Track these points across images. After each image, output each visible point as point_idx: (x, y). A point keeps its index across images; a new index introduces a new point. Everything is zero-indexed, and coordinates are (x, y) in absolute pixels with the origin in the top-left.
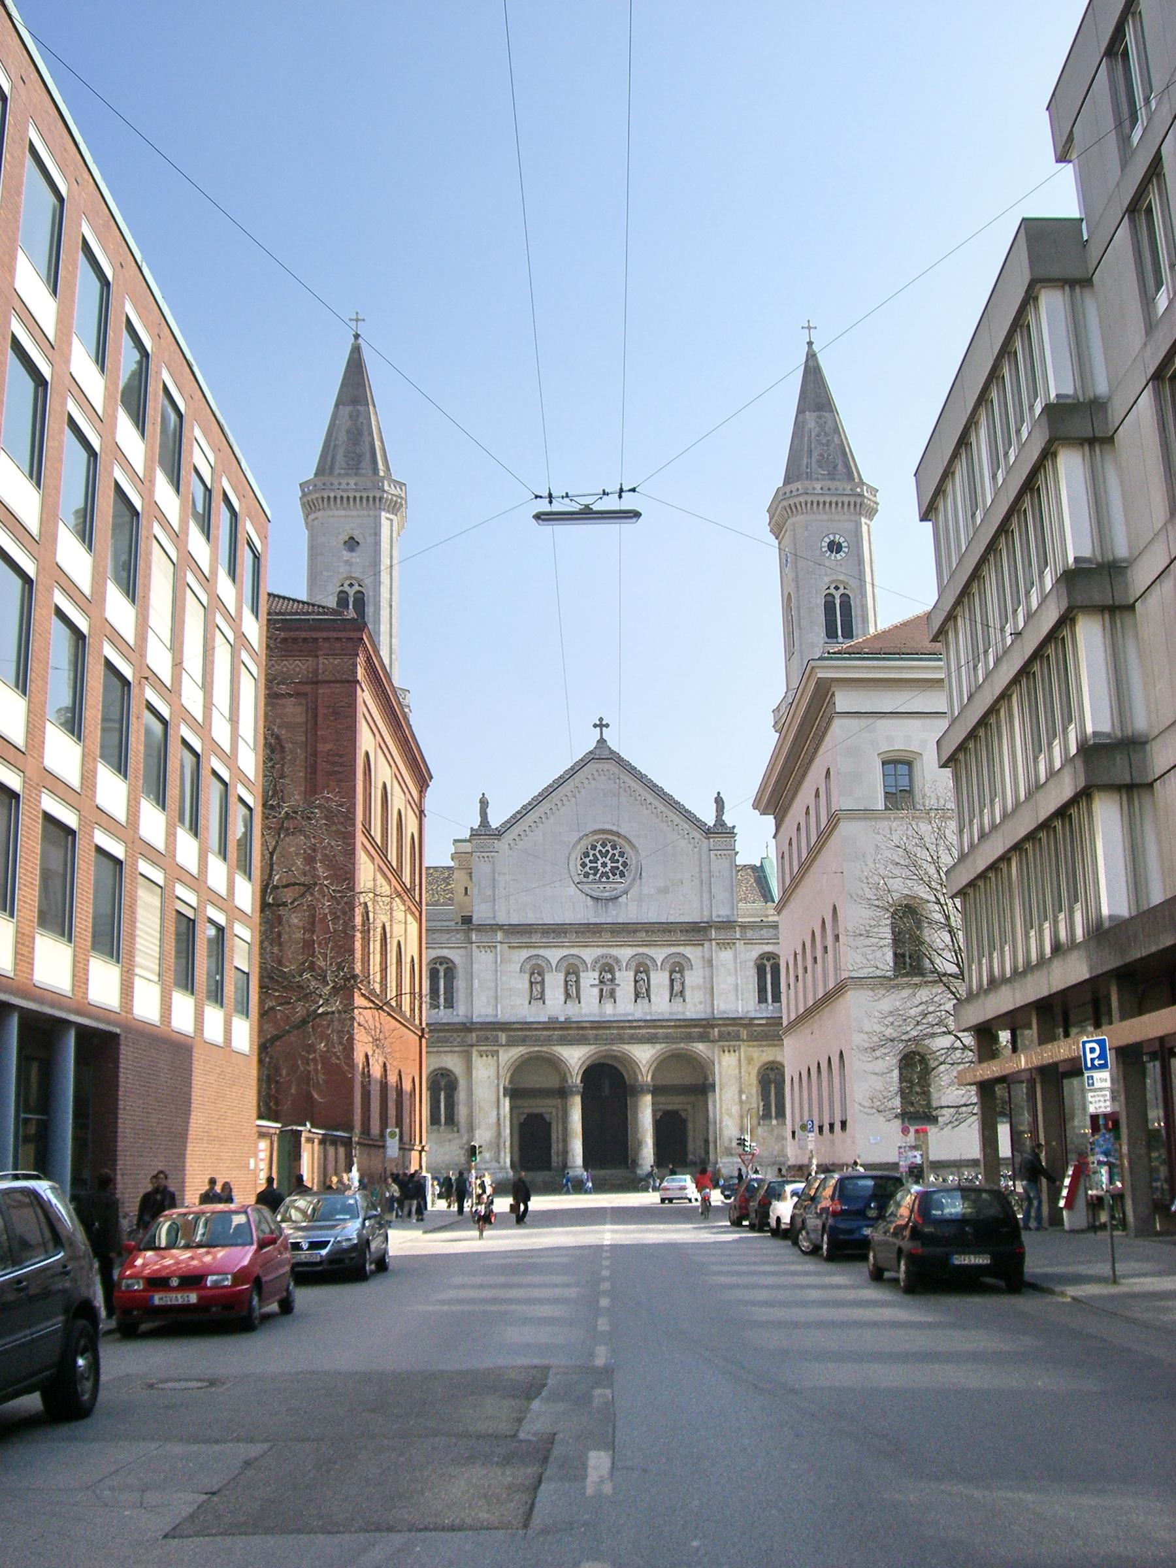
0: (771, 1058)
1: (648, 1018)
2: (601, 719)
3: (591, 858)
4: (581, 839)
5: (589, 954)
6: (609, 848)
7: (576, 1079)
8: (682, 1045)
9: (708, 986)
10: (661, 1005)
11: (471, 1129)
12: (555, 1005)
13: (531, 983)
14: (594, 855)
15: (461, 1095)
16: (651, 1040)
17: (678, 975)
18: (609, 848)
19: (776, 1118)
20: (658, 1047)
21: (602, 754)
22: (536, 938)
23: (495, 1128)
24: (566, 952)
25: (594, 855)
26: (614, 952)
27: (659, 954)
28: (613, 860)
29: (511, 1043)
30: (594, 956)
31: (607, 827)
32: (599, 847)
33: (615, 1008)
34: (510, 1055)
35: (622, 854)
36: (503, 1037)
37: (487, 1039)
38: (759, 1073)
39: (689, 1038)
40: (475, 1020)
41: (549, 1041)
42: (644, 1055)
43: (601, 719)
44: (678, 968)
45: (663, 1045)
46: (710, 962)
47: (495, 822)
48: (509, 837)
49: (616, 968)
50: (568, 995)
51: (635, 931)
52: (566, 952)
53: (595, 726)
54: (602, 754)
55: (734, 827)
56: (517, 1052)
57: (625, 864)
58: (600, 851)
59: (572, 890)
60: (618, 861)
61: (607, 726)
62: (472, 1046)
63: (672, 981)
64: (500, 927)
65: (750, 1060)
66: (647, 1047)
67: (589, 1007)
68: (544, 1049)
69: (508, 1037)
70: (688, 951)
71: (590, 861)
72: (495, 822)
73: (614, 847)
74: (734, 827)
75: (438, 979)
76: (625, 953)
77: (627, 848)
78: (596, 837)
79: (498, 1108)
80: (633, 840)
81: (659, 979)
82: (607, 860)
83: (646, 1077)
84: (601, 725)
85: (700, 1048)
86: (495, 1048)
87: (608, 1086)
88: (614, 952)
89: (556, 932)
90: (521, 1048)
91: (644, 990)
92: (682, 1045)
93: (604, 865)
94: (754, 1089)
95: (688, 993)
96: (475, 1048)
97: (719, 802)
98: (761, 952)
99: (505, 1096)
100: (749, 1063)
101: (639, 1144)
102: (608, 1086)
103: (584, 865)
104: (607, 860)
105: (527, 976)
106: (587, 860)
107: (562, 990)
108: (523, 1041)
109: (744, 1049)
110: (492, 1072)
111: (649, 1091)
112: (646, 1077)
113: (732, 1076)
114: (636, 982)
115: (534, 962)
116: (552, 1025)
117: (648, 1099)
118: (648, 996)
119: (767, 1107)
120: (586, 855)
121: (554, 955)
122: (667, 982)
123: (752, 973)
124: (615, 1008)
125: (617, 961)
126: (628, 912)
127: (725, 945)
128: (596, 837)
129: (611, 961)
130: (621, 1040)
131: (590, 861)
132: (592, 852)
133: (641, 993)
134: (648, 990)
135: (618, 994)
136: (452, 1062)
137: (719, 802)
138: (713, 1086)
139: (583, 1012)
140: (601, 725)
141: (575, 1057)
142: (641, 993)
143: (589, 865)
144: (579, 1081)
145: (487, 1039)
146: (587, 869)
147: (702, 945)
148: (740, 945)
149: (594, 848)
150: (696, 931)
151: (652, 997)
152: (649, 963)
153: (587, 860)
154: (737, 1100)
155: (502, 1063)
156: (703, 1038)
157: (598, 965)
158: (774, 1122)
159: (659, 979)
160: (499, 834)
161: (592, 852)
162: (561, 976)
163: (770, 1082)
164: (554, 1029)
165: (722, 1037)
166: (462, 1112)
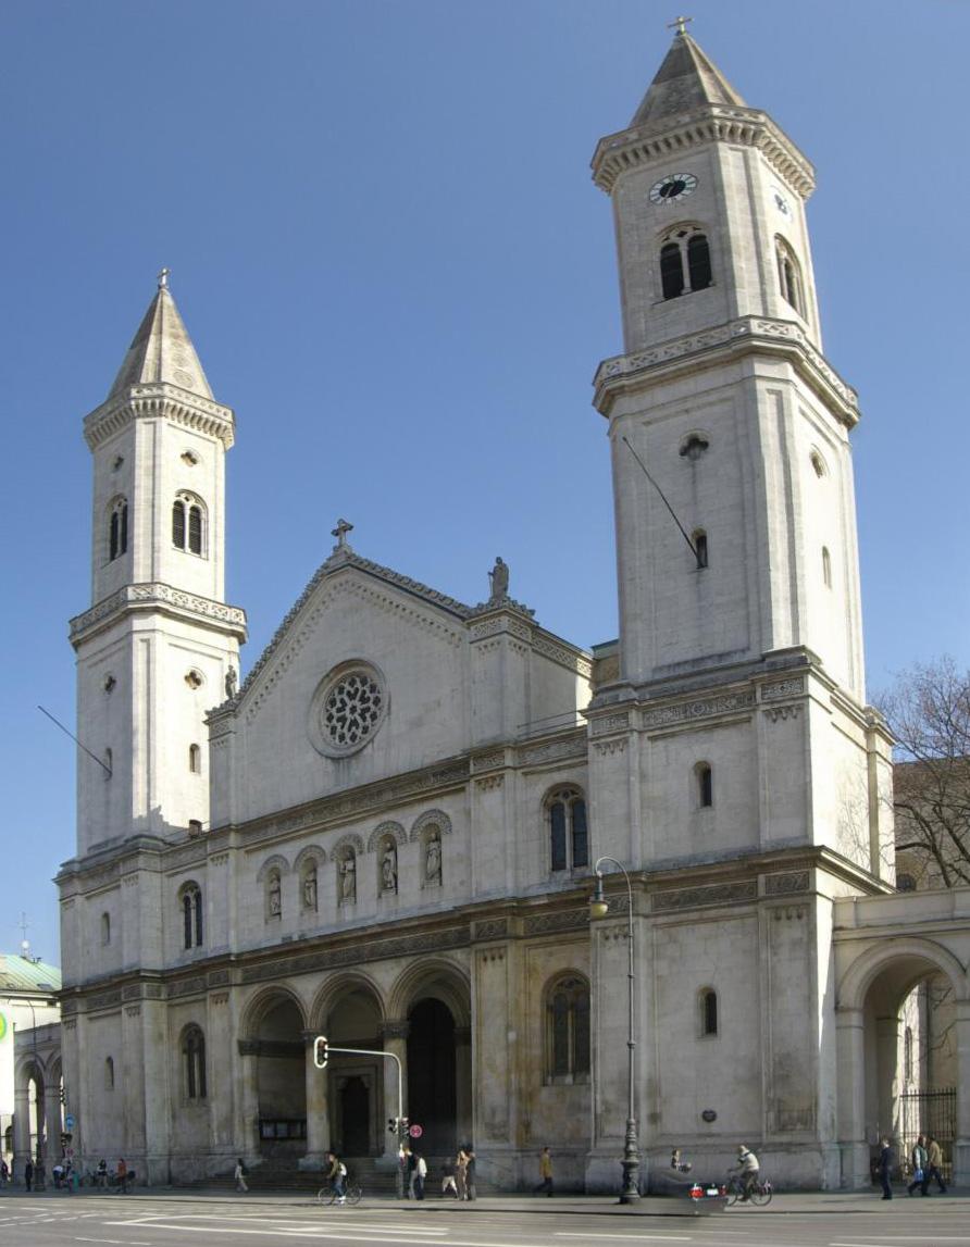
0: (564, 965)
3: (339, 705)
6: (358, 685)
8: (434, 957)
10: (413, 898)
14: (342, 701)
18: (358, 685)
20: (404, 962)
22: (272, 831)
29: (246, 983)
33: (355, 911)
38: (547, 989)
39: (446, 944)
41: (284, 973)
44: (434, 834)
45: (410, 959)
49: (357, 851)
50: (307, 905)
51: (380, 793)
59: (311, 756)
65: (530, 971)
66: (389, 964)
67: (330, 917)
68: (278, 984)
70: (448, 805)
73: (364, 682)
81: (410, 857)
85: (459, 957)
97: (500, 574)
103: (330, 718)
109: (513, 951)
118: (396, 886)
124: (355, 911)
125: (358, 840)
132: (338, 698)
137: (500, 574)
139: (322, 922)
149: (341, 690)
151: (399, 885)
156: (463, 941)
165: (482, 937)
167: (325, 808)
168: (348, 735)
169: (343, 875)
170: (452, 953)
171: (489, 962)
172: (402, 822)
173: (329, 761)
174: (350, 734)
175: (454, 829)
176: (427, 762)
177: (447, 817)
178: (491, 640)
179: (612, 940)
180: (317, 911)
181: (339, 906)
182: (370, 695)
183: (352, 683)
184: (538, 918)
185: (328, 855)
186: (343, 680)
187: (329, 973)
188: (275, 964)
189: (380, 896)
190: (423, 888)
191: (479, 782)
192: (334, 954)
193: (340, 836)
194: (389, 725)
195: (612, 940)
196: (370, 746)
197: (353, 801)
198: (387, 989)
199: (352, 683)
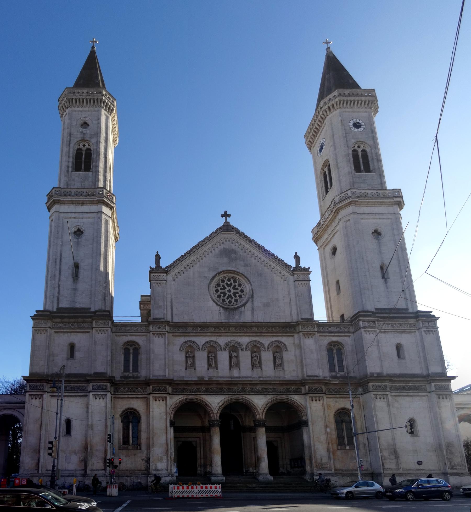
1: (261, 379)
2: (226, 212)
4: (216, 275)
5: (222, 341)
6: (232, 281)
7: (216, 416)
8: (284, 396)
9: (299, 361)
11: (149, 447)
12: (201, 369)
13: (187, 358)
14: (223, 286)
15: (143, 425)
16: (264, 393)
17: (279, 354)
18: (232, 281)
19: (348, 445)
20: (269, 397)
21: (227, 228)
22: (189, 330)
23: (165, 446)
24: (208, 339)
25: (223, 286)
26: (239, 339)
27: (266, 341)
28: (234, 288)
30: (225, 342)
31: (230, 269)
32: (226, 281)
33: (239, 373)
34: (175, 400)
35: (240, 285)
36: (169, 389)
37: (159, 389)
39: (289, 392)
40: (151, 378)
41: (198, 392)
42: (260, 402)
43: (226, 212)
44: (278, 350)
45: (272, 396)
46: (299, 346)
47: (164, 264)
48: (173, 273)
50: (209, 365)
52: (208, 339)
53: (222, 216)
54: (227, 228)
55: (309, 268)
56: (177, 399)
57: (242, 291)
58: (227, 284)
59: (211, 303)
60: (237, 289)
61: (229, 216)
62: (149, 394)
63: (274, 358)
64: (168, 323)
66: (261, 397)
69: (173, 389)
70: (284, 340)
71: (221, 289)
72: (164, 264)
73: (235, 281)
74: (309, 268)
75: (129, 354)
76: (245, 340)
77: (243, 281)
78: (224, 275)
79: (167, 433)
80: (248, 276)
81: (267, 357)
82: (231, 288)
83: (261, 415)
84: (226, 215)
86: (165, 395)
87: (235, 421)
88: (239, 339)
89: (202, 328)
90: (181, 396)
91: (257, 363)
92: (284, 396)
93: (229, 291)
94: (333, 426)
95: (286, 365)
96: (151, 396)
98: (330, 341)
99: (170, 426)
100: (328, 409)
101: (258, 460)
102: (235, 421)
103: (217, 291)
104: (233, 291)
105: (184, 353)
106: (219, 288)
107: (206, 361)
108: (182, 392)
110: (163, 409)
111: (264, 425)
112: (261, 415)
113: (318, 413)
114: (252, 358)
115: (188, 344)
116: (201, 382)
117: (262, 431)
119: (340, 437)
120: (218, 285)
121: (201, 341)
122: (272, 358)
123: (325, 353)
124: (239, 373)
125: (240, 345)
126: (246, 316)
127: (307, 335)
128: (224, 275)
130: (244, 392)
131: (221, 289)
132: (222, 284)
133: (256, 363)
134: (260, 363)
135: (242, 365)
136: (137, 405)
138: (306, 423)
139: (220, 375)
140: (226, 215)
141: (215, 402)
142: (256, 363)
143: (220, 291)
144: (218, 418)
145: (159, 389)
146: (219, 293)
147: (293, 336)
148: (317, 335)
149: (223, 281)
150: (288, 328)
151: (263, 367)
152: (260, 346)
153: (219, 288)
154: (323, 432)
155: (168, 404)
156: (298, 392)
157: (228, 348)
158: (348, 448)
159: (267, 357)
160: (167, 271)
161: (222, 284)
162: (205, 353)
163: (342, 421)
164: (201, 384)
165: (311, 391)
166: (143, 436)
167: (221, 327)
168: (227, 301)
169: (230, 358)
170: (292, 396)
171: (314, 401)
172: (263, 342)
173: (221, 308)
174: (228, 300)
175: (289, 349)
176: (273, 321)
177: (285, 345)
178: (304, 282)
179: (378, 399)
180: (217, 369)
181: (230, 369)
182: (221, 286)
183: (229, 280)
184: (331, 388)
185: (222, 347)
186: (225, 278)
187: (227, 396)
188: (194, 388)
189: (252, 369)
190: (274, 369)
191: (304, 334)
192: (229, 389)
194: (253, 301)
195: (378, 399)
196: (243, 307)
198: (260, 407)
199: (229, 280)
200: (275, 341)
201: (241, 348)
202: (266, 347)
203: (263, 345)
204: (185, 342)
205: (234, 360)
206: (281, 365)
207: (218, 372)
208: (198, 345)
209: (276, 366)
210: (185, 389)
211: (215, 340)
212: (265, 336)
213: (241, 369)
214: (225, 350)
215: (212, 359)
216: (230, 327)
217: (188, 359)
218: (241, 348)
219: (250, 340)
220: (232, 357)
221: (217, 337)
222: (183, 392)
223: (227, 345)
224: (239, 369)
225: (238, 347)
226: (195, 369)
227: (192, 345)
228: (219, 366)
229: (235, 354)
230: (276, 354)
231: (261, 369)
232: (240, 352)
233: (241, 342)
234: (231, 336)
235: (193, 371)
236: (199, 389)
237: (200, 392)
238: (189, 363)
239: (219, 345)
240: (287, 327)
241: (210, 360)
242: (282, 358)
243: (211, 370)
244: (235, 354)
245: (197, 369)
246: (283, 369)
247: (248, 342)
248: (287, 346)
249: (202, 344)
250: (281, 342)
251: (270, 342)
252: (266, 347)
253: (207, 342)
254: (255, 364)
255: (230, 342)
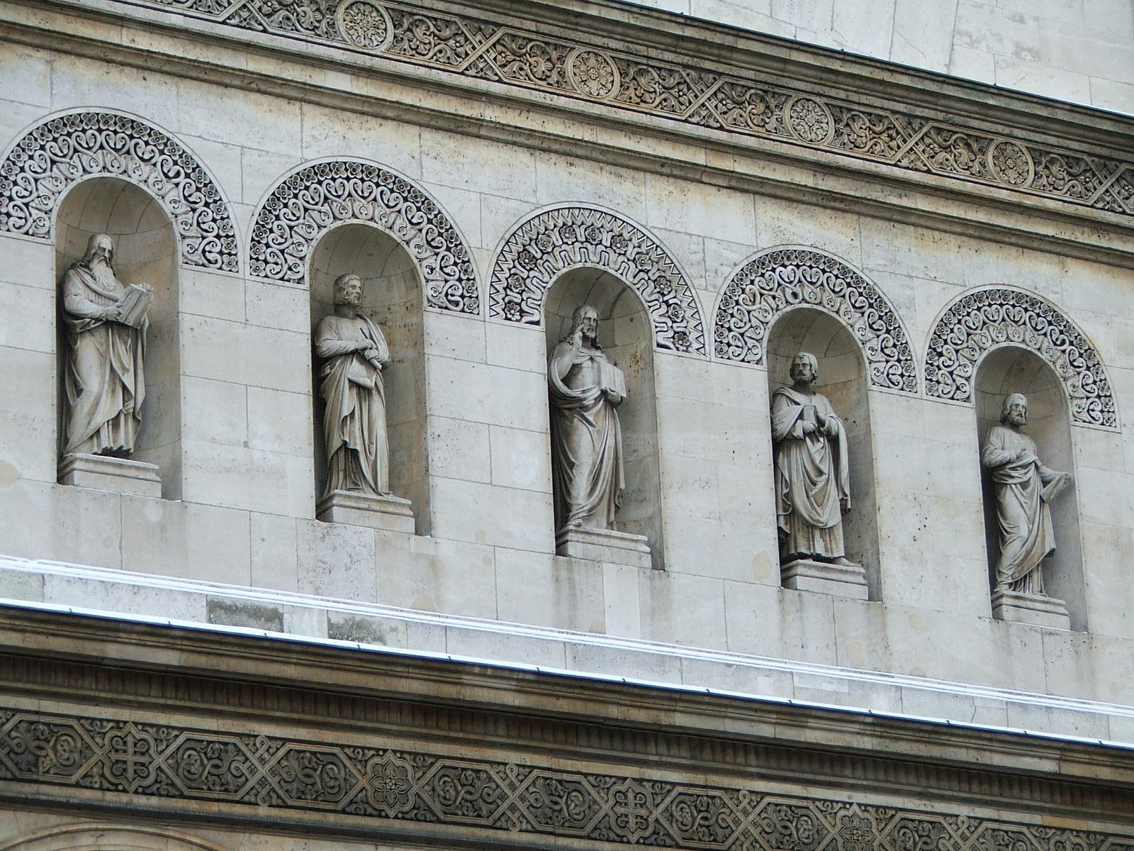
13: (68, 328)
50: (334, 465)
88: (651, 207)
91: (830, 515)
95: (1100, 574)
115: (96, 165)
129: (618, 267)
152: (856, 325)
157: (540, 284)
169: (562, 409)
172: (889, 289)
180: (423, 527)
181: (560, 547)
185: (483, 270)
190: (997, 614)
193: (547, 201)
197: (631, 68)
200: (1001, 296)
201: (673, 314)
202: (919, 348)
203: (886, 320)
204: (63, 130)
205: (592, 442)
206: (1049, 567)
207: (434, 564)
208: (212, 198)
209: (1008, 571)
210: (57, 729)
211: (410, 175)
212: (901, 216)
213: (673, 557)
214: (513, 310)
215: (363, 391)
216: (561, 47)
217: (88, 350)
218: (673, 314)
219: (768, 243)
220: (578, 406)
221: (430, 138)
222: (28, 771)
223: (526, 251)
224: (658, 563)
225: (646, 294)
226: (171, 489)
227: (141, 175)
228: (449, 493)
229: (602, 375)
230: (1007, 445)
231: (874, 595)
232: (665, 361)
233: (676, 248)
234: (570, 150)
235: (154, 511)
236: (218, 751)
237: (228, 789)
238: (99, 402)
239: (446, 237)
240: (1107, 164)
241: (348, 401)
242: (1059, 499)
243: (355, 526)
244: (614, 379)
245: (194, 485)
246: (1079, 625)
247: (741, 258)
248: (1115, 374)
249: (258, 196)
250: (1056, 318)
251: (954, 295)
252: (919, 348)
253: (319, 171)
254: (810, 527)
255: (574, 225)
